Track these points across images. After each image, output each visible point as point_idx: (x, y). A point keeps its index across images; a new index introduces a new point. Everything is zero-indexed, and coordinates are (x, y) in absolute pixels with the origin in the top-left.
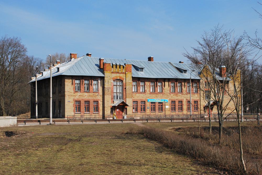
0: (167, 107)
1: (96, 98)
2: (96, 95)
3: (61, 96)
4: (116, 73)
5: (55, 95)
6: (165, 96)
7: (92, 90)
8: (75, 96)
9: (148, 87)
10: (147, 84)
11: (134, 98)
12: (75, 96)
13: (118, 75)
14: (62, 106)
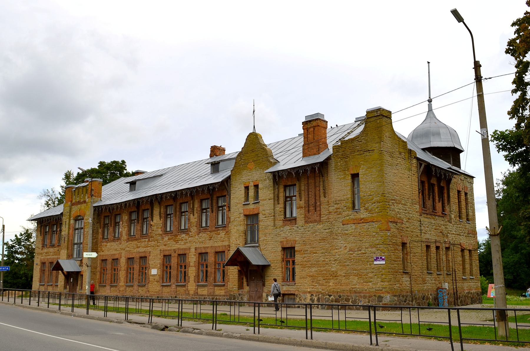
0: (154, 272)
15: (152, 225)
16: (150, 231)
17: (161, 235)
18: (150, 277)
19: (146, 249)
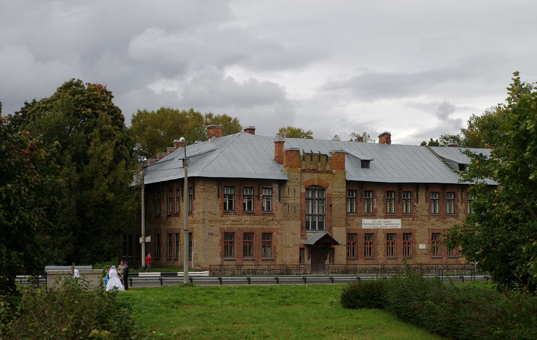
1: (270, 227)
2: (269, 221)
3: (193, 221)
4: (311, 173)
5: (178, 218)
6: (418, 222)
7: (259, 208)
8: (223, 222)
9: (382, 202)
10: (378, 195)
11: (348, 227)
12: (223, 222)
13: (316, 175)
14: (195, 243)
15: (415, 206)
16: (414, 212)
17: (428, 216)
18: (417, 251)
19: (411, 226)
